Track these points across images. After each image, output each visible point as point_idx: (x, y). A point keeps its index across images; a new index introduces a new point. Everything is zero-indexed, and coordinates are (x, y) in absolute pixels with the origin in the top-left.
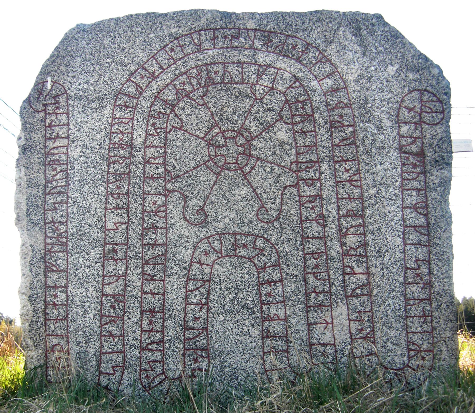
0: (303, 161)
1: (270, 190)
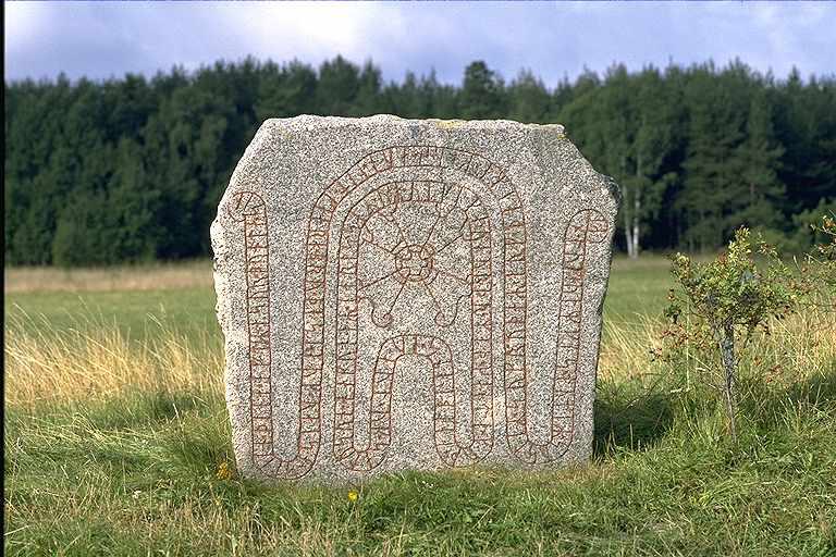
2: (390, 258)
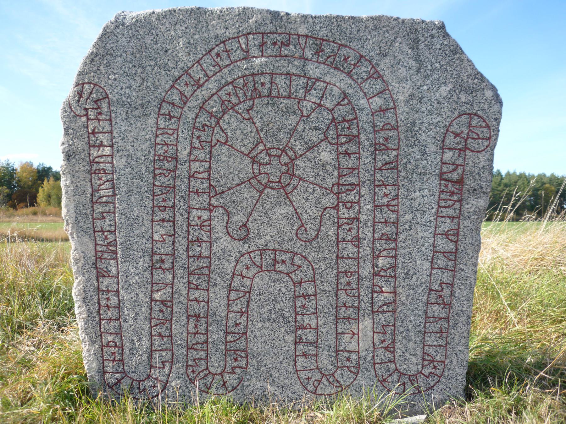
0: (345, 183)
1: (310, 210)
2: (247, 162)
